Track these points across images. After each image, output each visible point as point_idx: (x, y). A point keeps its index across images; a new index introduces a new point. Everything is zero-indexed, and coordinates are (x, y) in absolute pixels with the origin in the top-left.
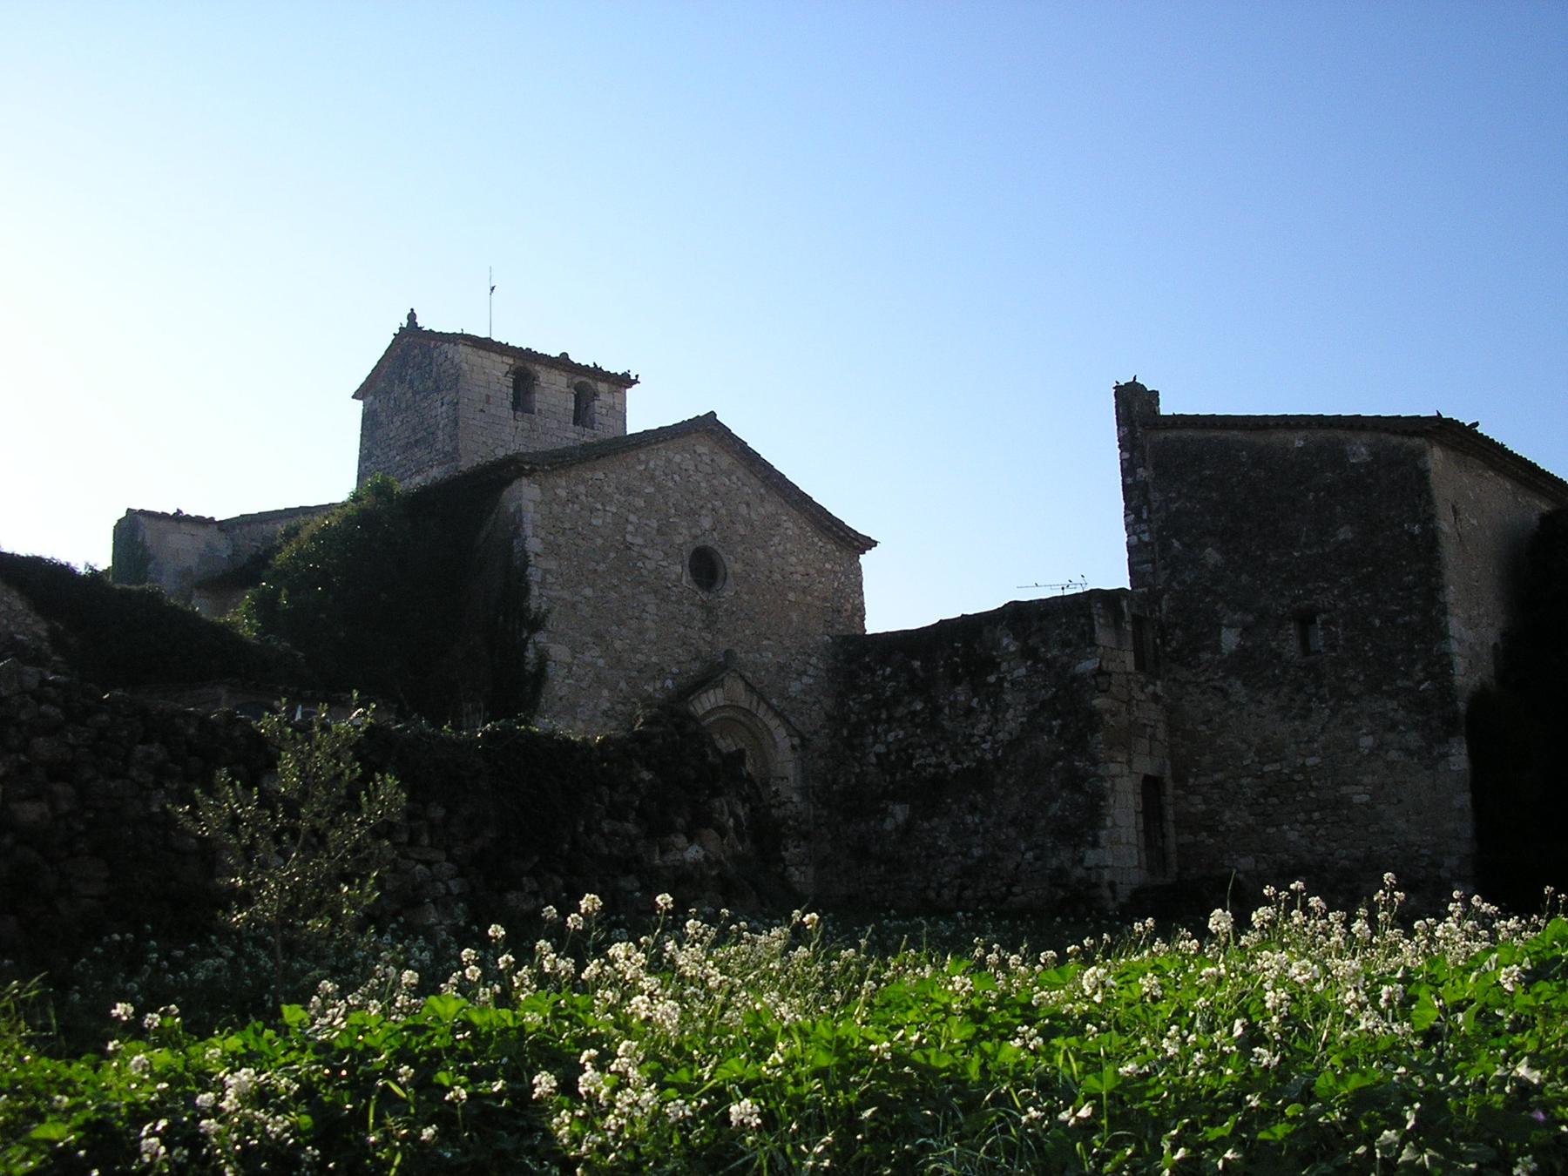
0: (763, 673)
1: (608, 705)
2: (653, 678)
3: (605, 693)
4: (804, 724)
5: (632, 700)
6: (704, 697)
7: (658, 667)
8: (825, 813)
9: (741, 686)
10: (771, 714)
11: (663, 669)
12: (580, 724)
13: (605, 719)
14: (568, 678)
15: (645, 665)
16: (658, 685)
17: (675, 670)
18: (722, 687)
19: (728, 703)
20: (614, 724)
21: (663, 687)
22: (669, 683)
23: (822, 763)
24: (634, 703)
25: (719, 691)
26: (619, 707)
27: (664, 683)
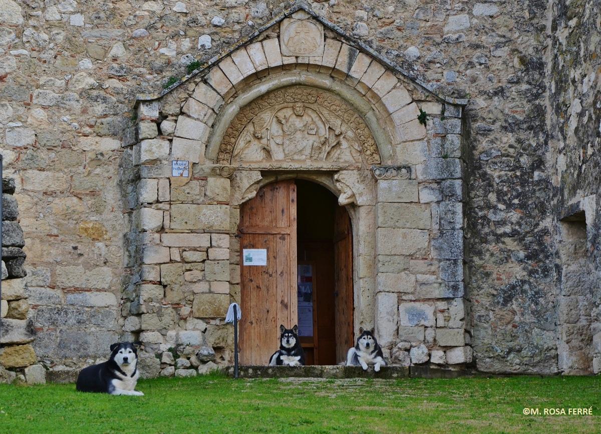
0: (391, 8)
1: (92, 81)
2: (175, 36)
3: (87, 64)
4: (474, 80)
5: (137, 70)
6: (240, 57)
7: (188, 18)
8: (514, 216)
9: (315, 32)
10: (378, 70)
11: (194, 21)
12: (39, 114)
13: (86, 103)
14: (15, 47)
15: (161, 18)
16: (186, 44)
17: (218, 20)
18: (278, 37)
19: (292, 60)
20: (99, 108)
21: (193, 48)
22: (205, 40)
23: (509, 138)
24: (140, 75)
25: (271, 45)
26: (115, 83)
27: (195, 40)
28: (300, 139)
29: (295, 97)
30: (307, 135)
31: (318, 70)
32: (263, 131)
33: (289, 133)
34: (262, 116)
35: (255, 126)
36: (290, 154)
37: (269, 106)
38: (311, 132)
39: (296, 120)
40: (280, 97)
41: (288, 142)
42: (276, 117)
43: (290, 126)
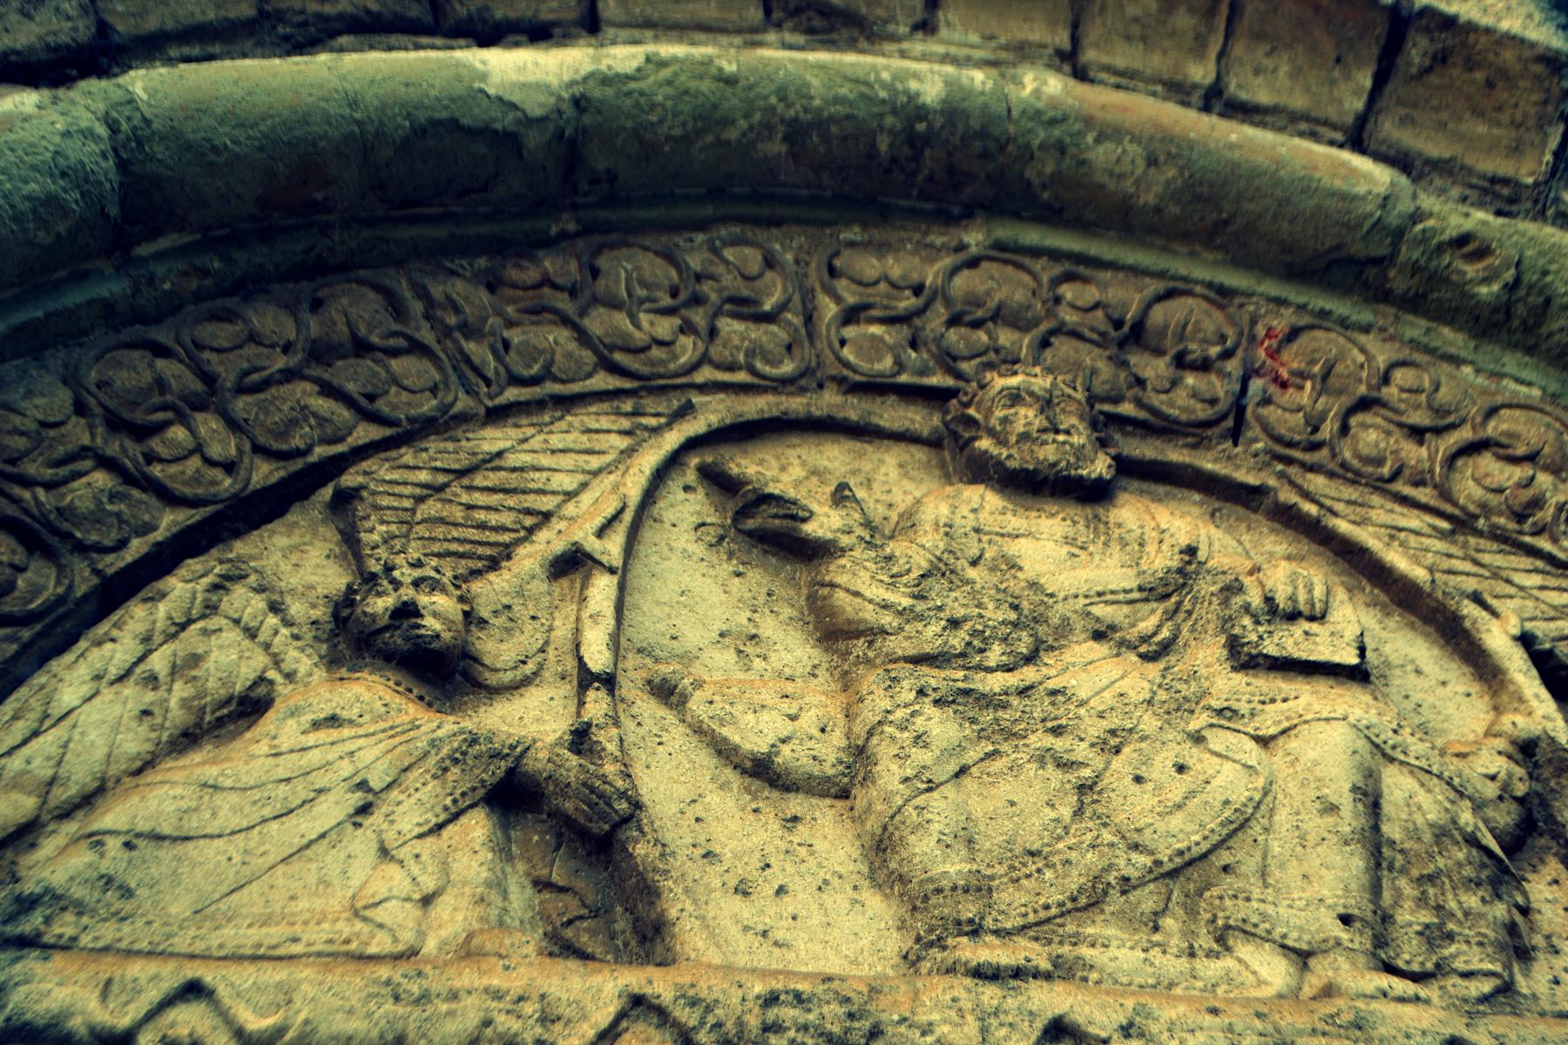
28: (1149, 723)
29: (955, 338)
30: (1229, 685)
31: (1201, 73)
32: (491, 589)
33: (930, 636)
34: (492, 439)
35: (374, 533)
36: (1013, 902)
37: (602, 381)
38: (1290, 641)
39: (1015, 522)
40: (745, 308)
41: (941, 726)
42: (719, 482)
43: (939, 569)
